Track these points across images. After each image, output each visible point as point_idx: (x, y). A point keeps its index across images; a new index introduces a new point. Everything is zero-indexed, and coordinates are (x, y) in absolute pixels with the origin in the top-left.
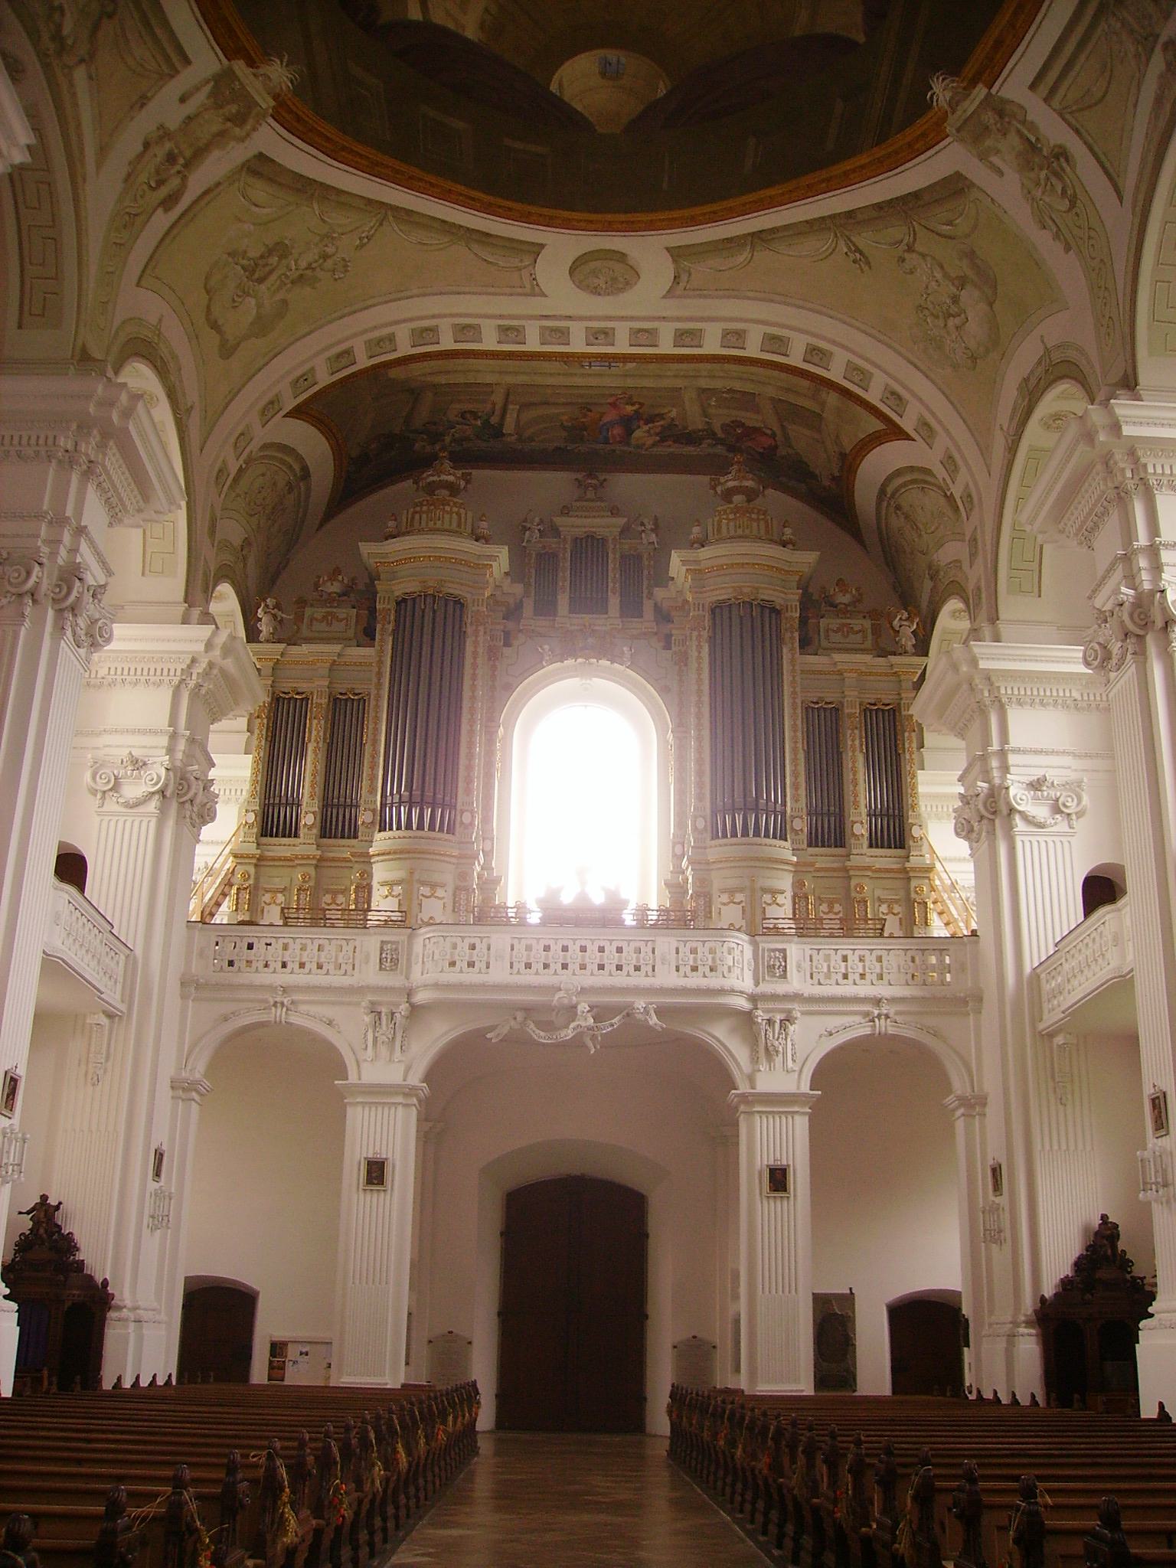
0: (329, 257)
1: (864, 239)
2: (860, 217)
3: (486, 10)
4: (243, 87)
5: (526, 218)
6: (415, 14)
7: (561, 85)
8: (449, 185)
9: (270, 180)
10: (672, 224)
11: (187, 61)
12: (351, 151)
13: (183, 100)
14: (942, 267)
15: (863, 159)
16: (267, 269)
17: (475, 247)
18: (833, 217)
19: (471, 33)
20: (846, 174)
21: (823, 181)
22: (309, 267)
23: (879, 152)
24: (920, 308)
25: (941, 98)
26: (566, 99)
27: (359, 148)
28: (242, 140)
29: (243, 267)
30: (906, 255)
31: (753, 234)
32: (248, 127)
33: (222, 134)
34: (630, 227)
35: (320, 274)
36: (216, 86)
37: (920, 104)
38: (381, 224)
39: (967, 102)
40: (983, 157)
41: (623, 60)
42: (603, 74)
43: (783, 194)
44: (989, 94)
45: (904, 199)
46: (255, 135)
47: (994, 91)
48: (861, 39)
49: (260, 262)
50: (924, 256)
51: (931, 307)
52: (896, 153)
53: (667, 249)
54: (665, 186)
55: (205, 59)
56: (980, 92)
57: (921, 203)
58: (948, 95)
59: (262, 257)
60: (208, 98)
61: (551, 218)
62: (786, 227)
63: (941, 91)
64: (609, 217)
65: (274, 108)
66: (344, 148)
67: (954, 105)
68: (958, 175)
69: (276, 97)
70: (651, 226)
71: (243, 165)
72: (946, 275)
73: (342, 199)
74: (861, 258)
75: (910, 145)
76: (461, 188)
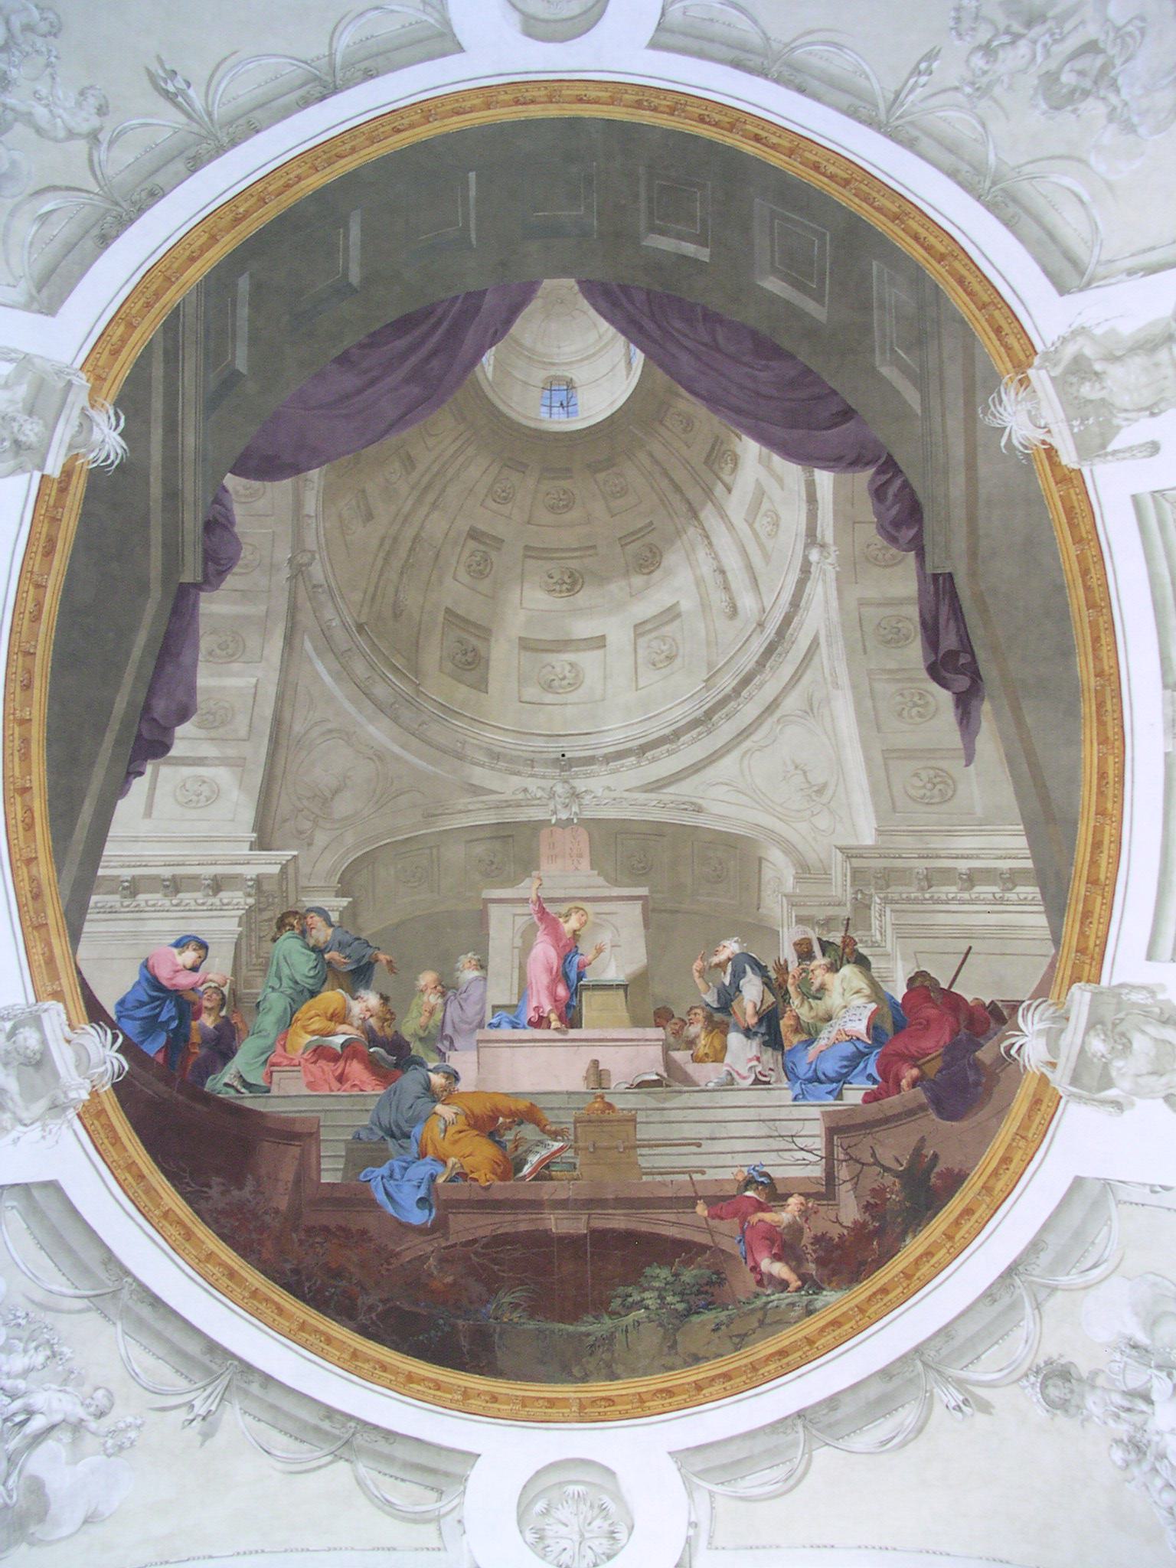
0: (980, 47)
1: (167, 123)
2: (179, 166)
3: (729, 491)
4: (1069, 420)
5: (679, 102)
6: (824, 479)
7: (629, 363)
8: (794, 168)
9: (1051, 236)
10: (455, 103)
11: (1136, 500)
12: (928, 249)
13: (1154, 448)
14: (39, 131)
15: (196, 273)
16: (1078, 64)
17: (755, 39)
18: (221, 150)
19: (750, 449)
20: (214, 239)
21: (246, 215)
22: (1016, 37)
23: (172, 297)
24: (55, 32)
25: (106, 430)
26: (622, 339)
27: (918, 253)
28: (1082, 331)
29: (1118, 91)
30: (96, 122)
31: (336, 90)
32: (1070, 350)
33: (1112, 358)
34: (519, 91)
35: (1002, 21)
36: (1104, 446)
37: (131, 403)
38: (897, 94)
39: (67, 439)
40: (25, 361)
41: (544, 414)
42: (570, 386)
43: (299, 178)
44: (41, 468)
45: (124, 223)
46: (1064, 331)
47: (37, 475)
48: (231, 481)
49: (1087, 84)
50: (71, 135)
51: (40, 42)
52: (148, 305)
53: (461, 49)
54: (472, 175)
55: (1113, 490)
56: (54, 467)
57: (95, 232)
58: (97, 436)
59: (1086, 94)
60: (1119, 428)
61: (639, 105)
62: (286, 113)
63: (108, 440)
64: (553, 111)
65: (1030, 366)
66: (941, 258)
67: (86, 422)
68: (50, 309)
69: (1024, 382)
70: (488, 96)
71: (1088, 285)
72: (28, 118)
73: (949, 160)
74: (166, 87)
75: (131, 327)
76: (776, 159)
